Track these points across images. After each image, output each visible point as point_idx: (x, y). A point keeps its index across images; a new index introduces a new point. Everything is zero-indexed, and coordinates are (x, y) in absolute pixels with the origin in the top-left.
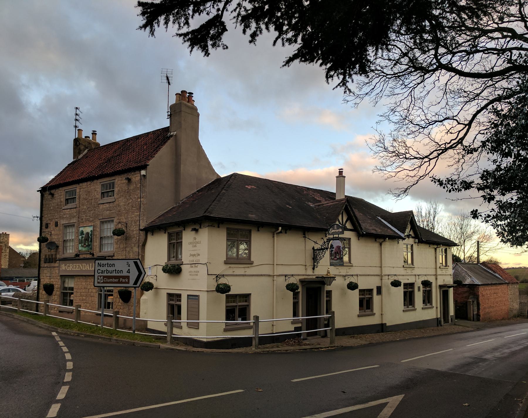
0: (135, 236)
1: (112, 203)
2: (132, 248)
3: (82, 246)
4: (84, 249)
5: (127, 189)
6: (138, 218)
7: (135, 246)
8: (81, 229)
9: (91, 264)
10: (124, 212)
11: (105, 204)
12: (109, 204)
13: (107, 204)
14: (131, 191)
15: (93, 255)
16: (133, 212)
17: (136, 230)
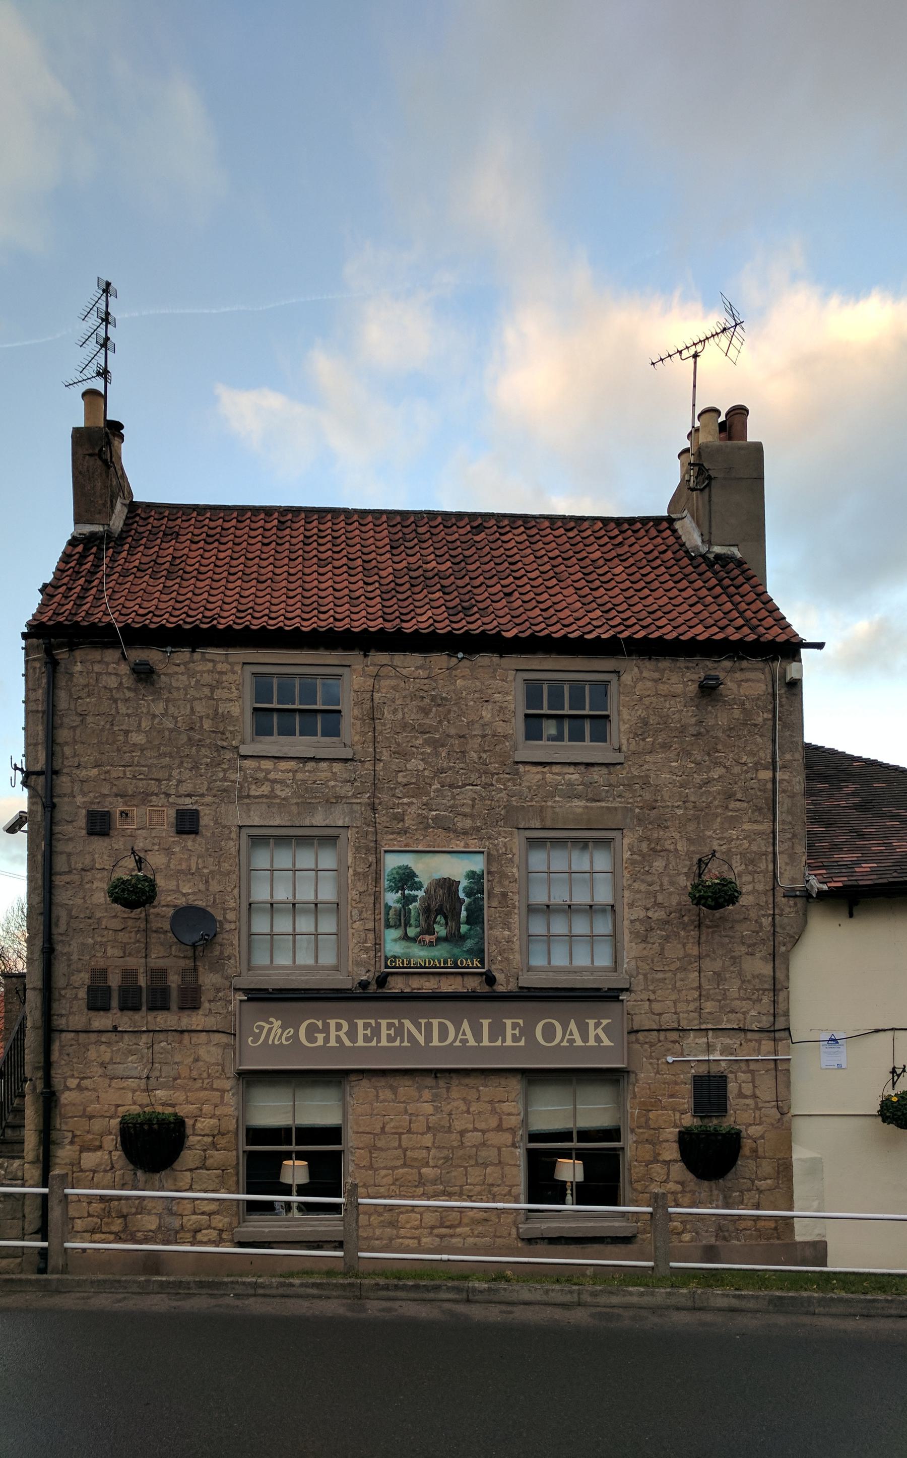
0: (753, 914)
1: (604, 770)
2: (735, 960)
3: (406, 937)
4: (419, 953)
5: (693, 720)
6: (761, 845)
7: (752, 954)
8: (392, 862)
9: (486, 1023)
10: (680, 812)
11: (556, 769)
12: (582, 768)
13: (571, 769)
14: (720, 734)
15: (490, 980)
16: (733, 822)
17: (754, 891)
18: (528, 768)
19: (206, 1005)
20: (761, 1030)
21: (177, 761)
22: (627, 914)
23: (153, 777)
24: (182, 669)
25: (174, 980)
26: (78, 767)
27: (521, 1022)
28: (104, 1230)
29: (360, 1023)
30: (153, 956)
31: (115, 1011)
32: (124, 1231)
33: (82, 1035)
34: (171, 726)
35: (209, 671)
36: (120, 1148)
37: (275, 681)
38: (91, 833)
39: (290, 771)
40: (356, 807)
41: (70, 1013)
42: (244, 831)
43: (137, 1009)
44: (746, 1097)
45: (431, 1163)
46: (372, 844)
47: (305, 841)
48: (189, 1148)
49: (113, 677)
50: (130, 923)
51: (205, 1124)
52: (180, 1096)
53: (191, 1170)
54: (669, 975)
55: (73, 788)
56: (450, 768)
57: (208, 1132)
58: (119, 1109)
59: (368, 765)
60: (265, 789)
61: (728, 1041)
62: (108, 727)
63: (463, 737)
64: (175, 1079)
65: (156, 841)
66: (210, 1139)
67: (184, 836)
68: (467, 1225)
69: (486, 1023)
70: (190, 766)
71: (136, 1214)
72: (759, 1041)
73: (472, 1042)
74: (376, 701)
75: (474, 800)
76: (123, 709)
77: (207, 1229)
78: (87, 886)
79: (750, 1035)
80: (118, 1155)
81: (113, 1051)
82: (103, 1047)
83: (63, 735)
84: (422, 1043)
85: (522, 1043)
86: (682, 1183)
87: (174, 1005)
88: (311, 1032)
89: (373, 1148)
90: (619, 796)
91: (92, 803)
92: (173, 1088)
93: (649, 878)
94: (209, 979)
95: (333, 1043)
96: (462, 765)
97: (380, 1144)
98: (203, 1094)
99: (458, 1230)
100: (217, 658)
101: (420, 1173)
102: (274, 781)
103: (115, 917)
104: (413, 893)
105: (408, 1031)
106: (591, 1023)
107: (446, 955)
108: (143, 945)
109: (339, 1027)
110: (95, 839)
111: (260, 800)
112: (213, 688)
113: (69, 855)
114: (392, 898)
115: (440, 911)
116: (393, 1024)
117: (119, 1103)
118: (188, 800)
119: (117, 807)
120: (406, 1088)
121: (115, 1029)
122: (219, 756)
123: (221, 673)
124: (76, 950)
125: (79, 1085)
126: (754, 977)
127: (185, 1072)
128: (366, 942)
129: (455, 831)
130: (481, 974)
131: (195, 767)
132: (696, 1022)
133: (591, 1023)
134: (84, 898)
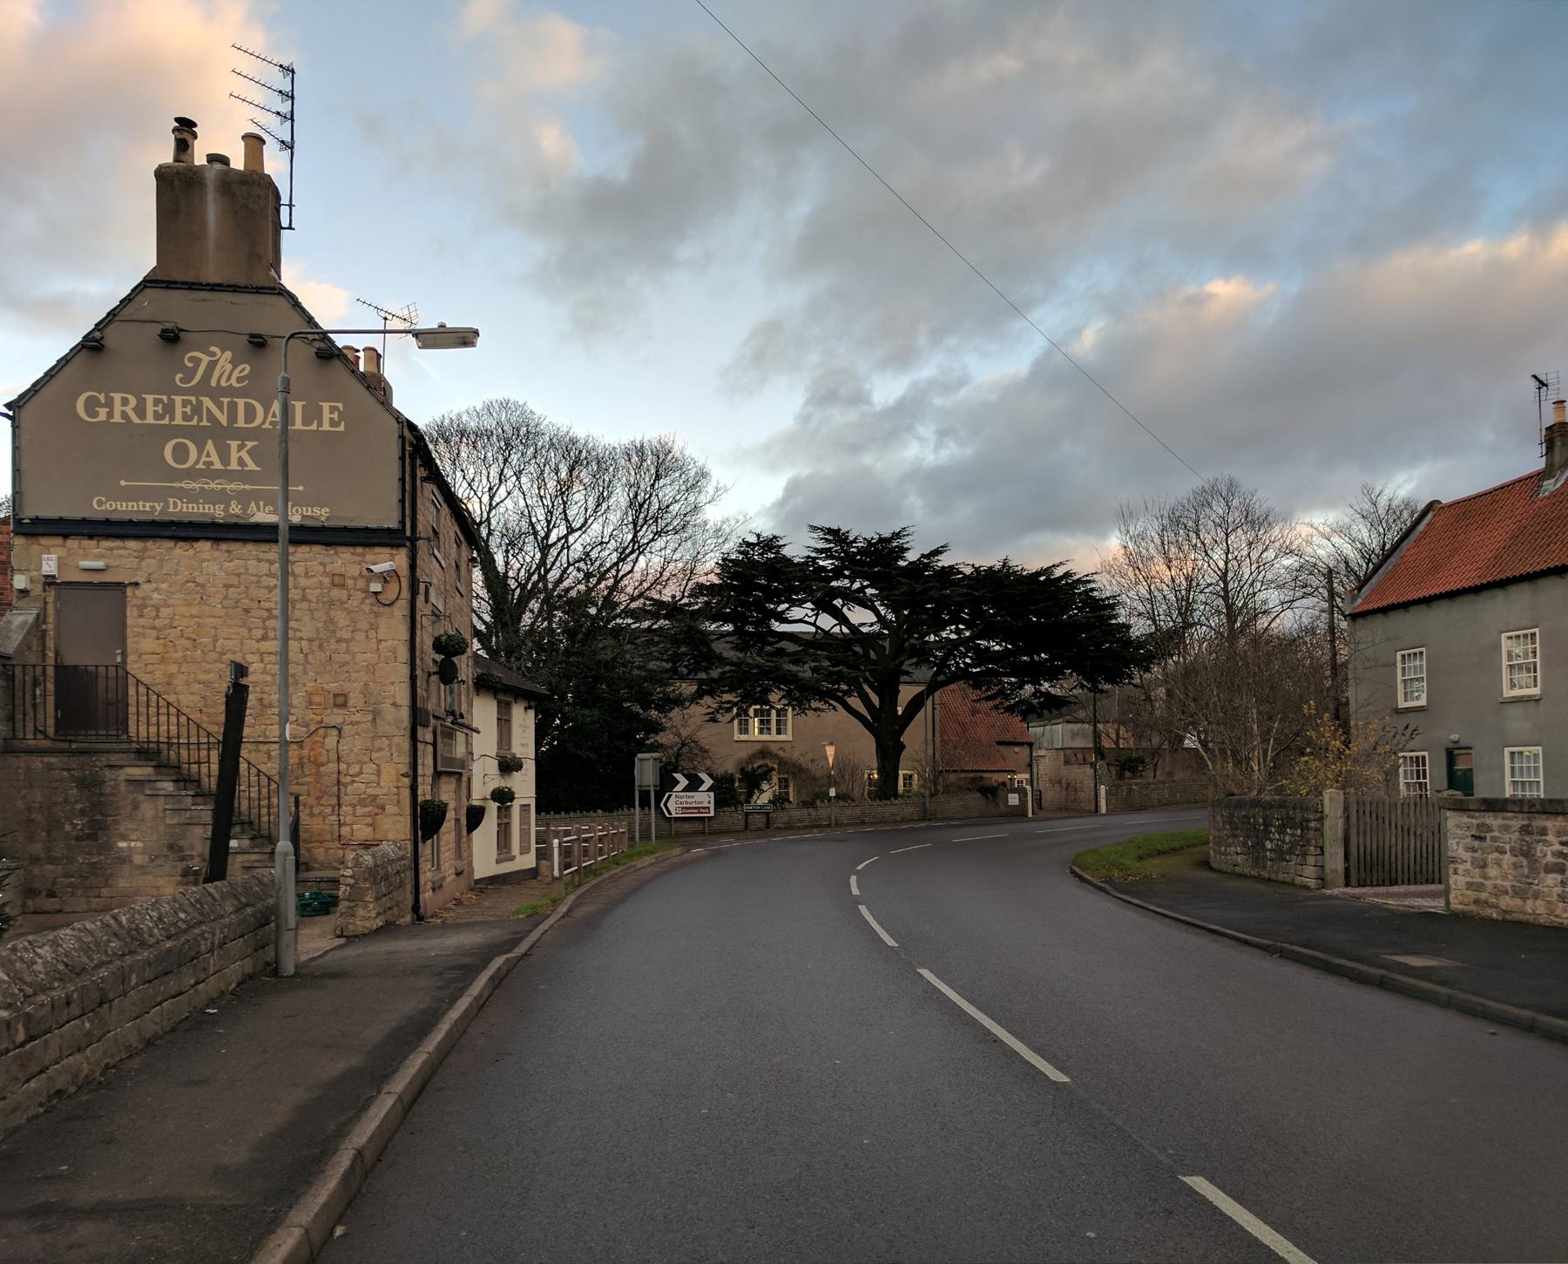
27: (340, 405)
29: (150, 398)
84: (225, 424)
85: (342, 428)
88: (91, 405)
95: (117, 418)
109: (125, 402)
116: (190, 402)
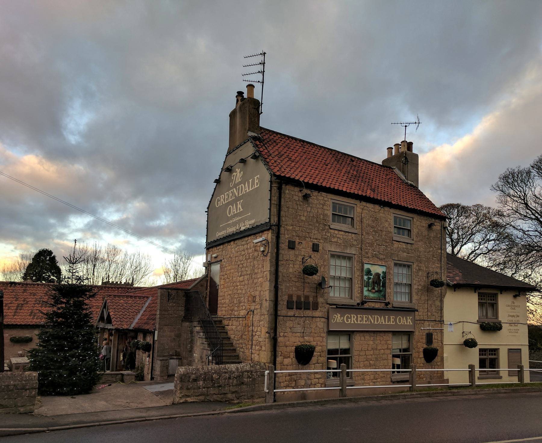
3: (368, 290)
4: (372, 295)
5: (427, 234)
7: (437, 300)
8: (366, 266)
11: (401, 243)
12: (406, 244)
13: (404, 244)
18: (395, 242)
19: (319, 308)
20: (439, 321)
21: (314, 227)
22: (415, 287)
23: (307, 231)
24: (315, 198)
25: (311, 299)
26: (286, 225)
27: (394, 317)
28: (290, 386)
30: (305, 291)
31: (294, 309)
32: (295, 386)
33: (285, 317)
34: (312, 216)
35: (322, 200)
36: (295, 357)
37: (338, 206)
38: (289, 248)
39: (342, 235)
40: (357, 249)
41: (282, 310)
42: (329, 252)
43: (301, 309)
44: (436, 339)
45: (372, 360)
46: (361, 261)
47: (344, 257)
48: (314, 357)
49: (297, 197)
50: (299, 279)
51: (318, 349)
52: (311, 339)
53: (314, 364)
54: (422, 305)
55: (284, 232)
56: (379, 240)
57: (319, 351)
58: (295, 343)
59: (360, 236)
60: (335, 240)
61: (432, 324)
62: (295, 213)
63: (381, 231)
64: (310, 333)
65: (307, 253)
66: (319, 354)
67: (314, 252)
68: (380, 378)
69: (387, 317)
70: (317, 229)
71: (298, 380)
72: (438, 324)
73: (384, 323)
74: (362, 216)
75: (384, 250)
76: (300, 208)
77: (318, 384)
78: (287, 266)
79: (437, 322)
80: (294, 359)
81: (293, 323)
82: (291, 322)
83: (282, 213)
85: (394, 323)
86: (423, 364)
87: (311, 308)
89: (359, 355)
90: (413, 253)
91: (290, 238)
92: (309, 336)
93: (418, 277)
94: (320, 300)
95: (352, 322)
96: (381, 239)
97: (361, 354)
98: (317, 338)
99: (378, 380)
100: (324, 196)
101: (370, 363)
102: (338, 238)
103: (295, 277)
104: (370, 276)
105: (370, 319)
106: (408, 317)
107: (377, 296)
108: (303, 287)
110: (290, 250)
111: (334, 243)
112: (323, 205)
113: (283, 255)
114: (365, 277)
115: (376, 283)
117: (295, 341)
118: (316, 241)
119: (297, 241)
120: (367, 337)
121: (294, 316)
122: (324, 227)
123: (325, 201)
124: (284, 288)
125: (283, 335)
126: (438, 306)
127: (313, 331)
128: (358, 291)
129: (379, 259)
130: (384, 302)
131: (318, 230)
132: (427, 318)
133: (408, 317)
134: (287, 270)
